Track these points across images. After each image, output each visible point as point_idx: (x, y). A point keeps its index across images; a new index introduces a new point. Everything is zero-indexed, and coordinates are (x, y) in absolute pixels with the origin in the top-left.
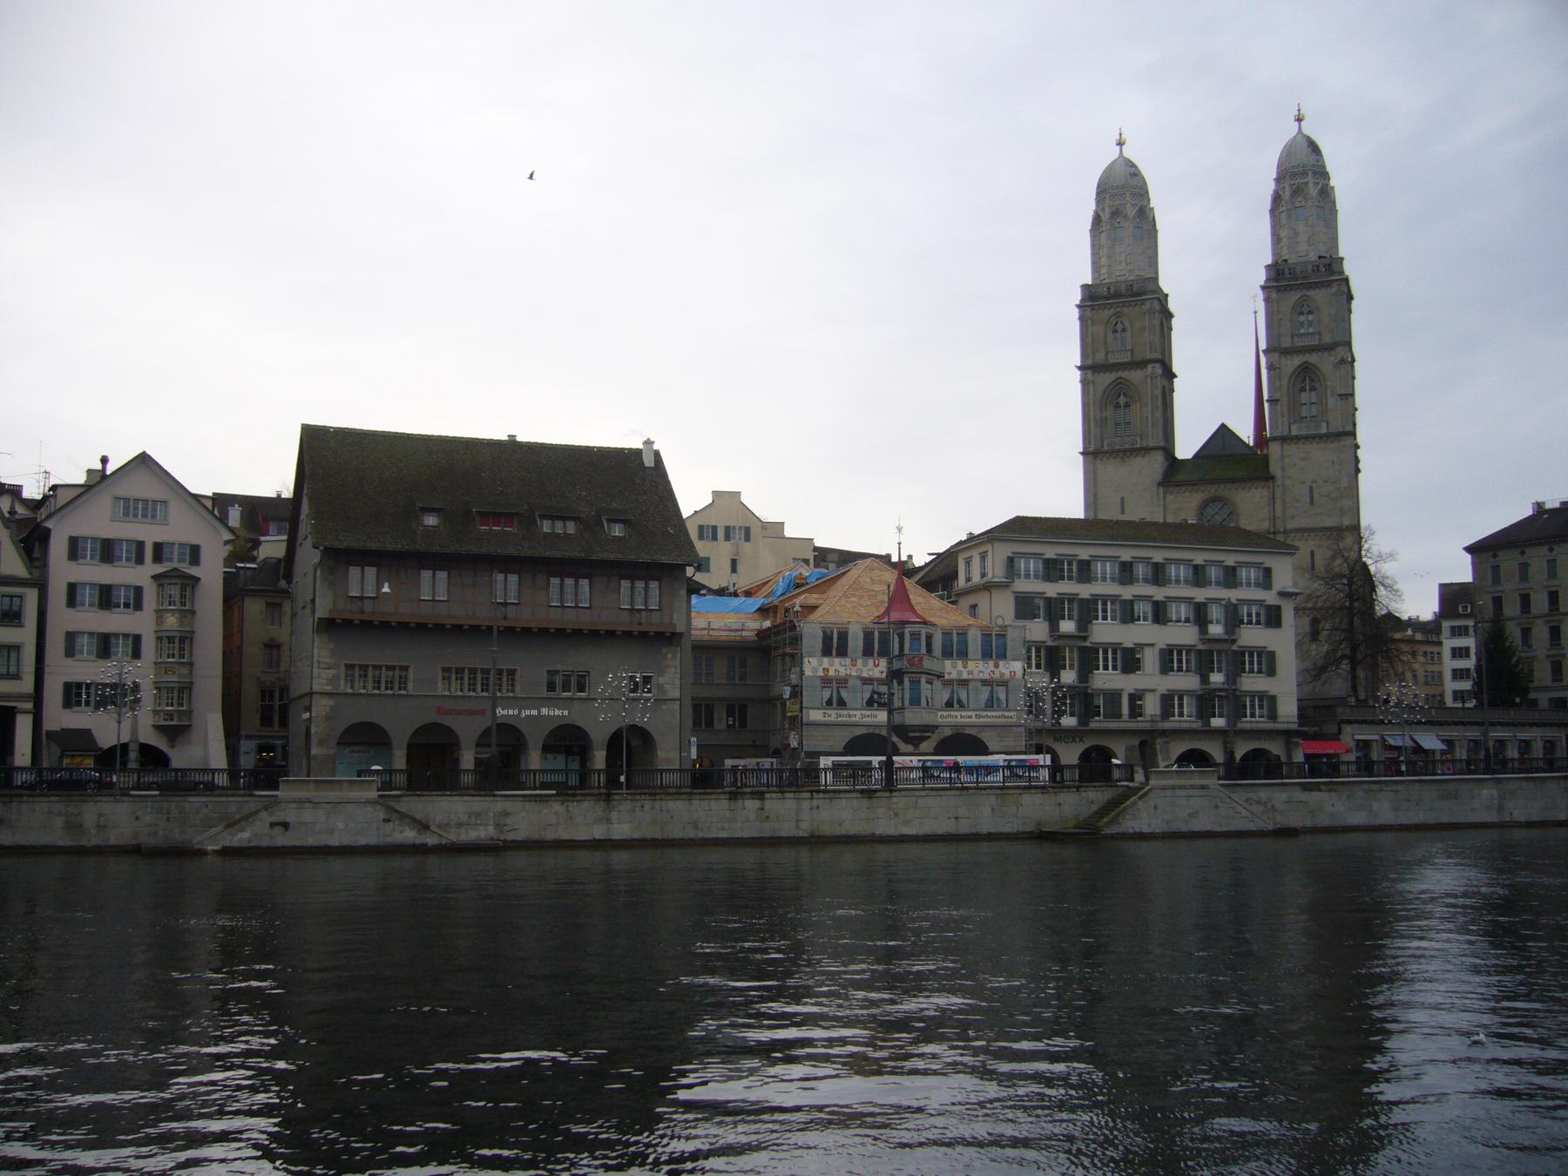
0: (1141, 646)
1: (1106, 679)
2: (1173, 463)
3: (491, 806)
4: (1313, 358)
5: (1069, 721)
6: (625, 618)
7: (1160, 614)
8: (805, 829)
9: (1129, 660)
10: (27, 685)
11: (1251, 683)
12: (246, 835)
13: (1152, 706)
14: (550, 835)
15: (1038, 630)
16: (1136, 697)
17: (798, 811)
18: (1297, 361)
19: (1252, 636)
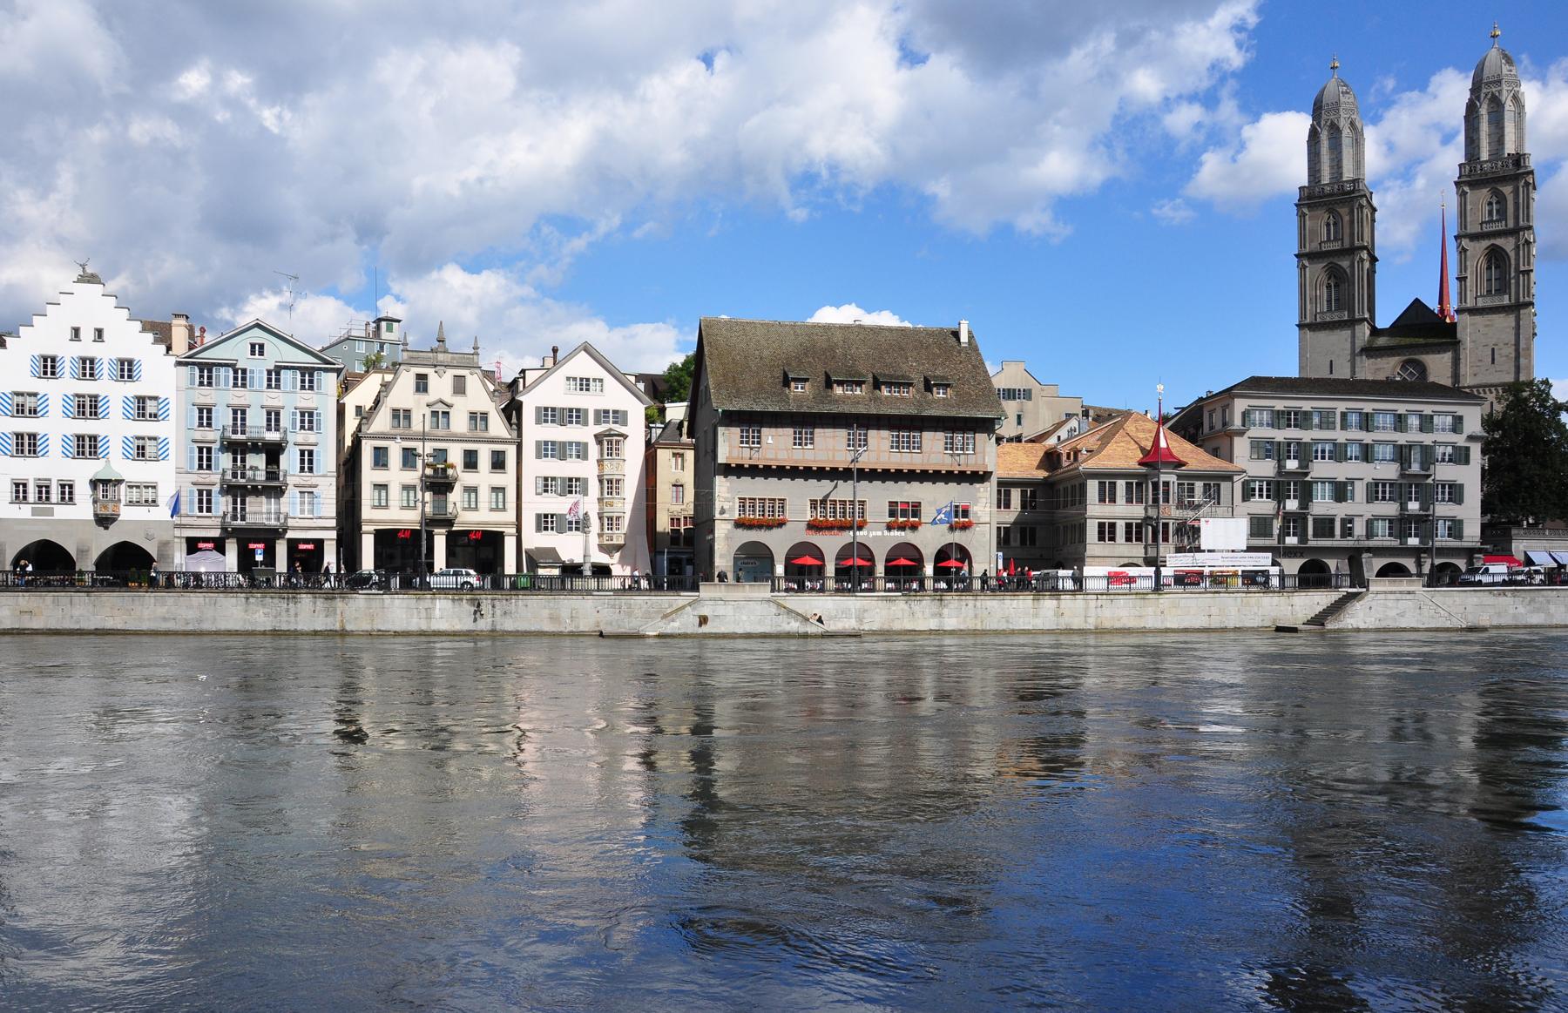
0: (1351, 481)
1: (1323, 504)
2: (1375, 332)
3: (852, 603)
4: (1499, 242)
5: (1292, 541)
6: (948, 460)
7: (1367, 454)
8: (1091, 624)
9: (1341, 491)
10: (510, 515)
11: (1443, 509)
12: (676, 624)
13: (1359, 528)
14: (897, 626)
15: (1267, 468)
16: (1348, 521)
17: (1087, 609)
18: (1486, 243)
19: (1444, 472)
